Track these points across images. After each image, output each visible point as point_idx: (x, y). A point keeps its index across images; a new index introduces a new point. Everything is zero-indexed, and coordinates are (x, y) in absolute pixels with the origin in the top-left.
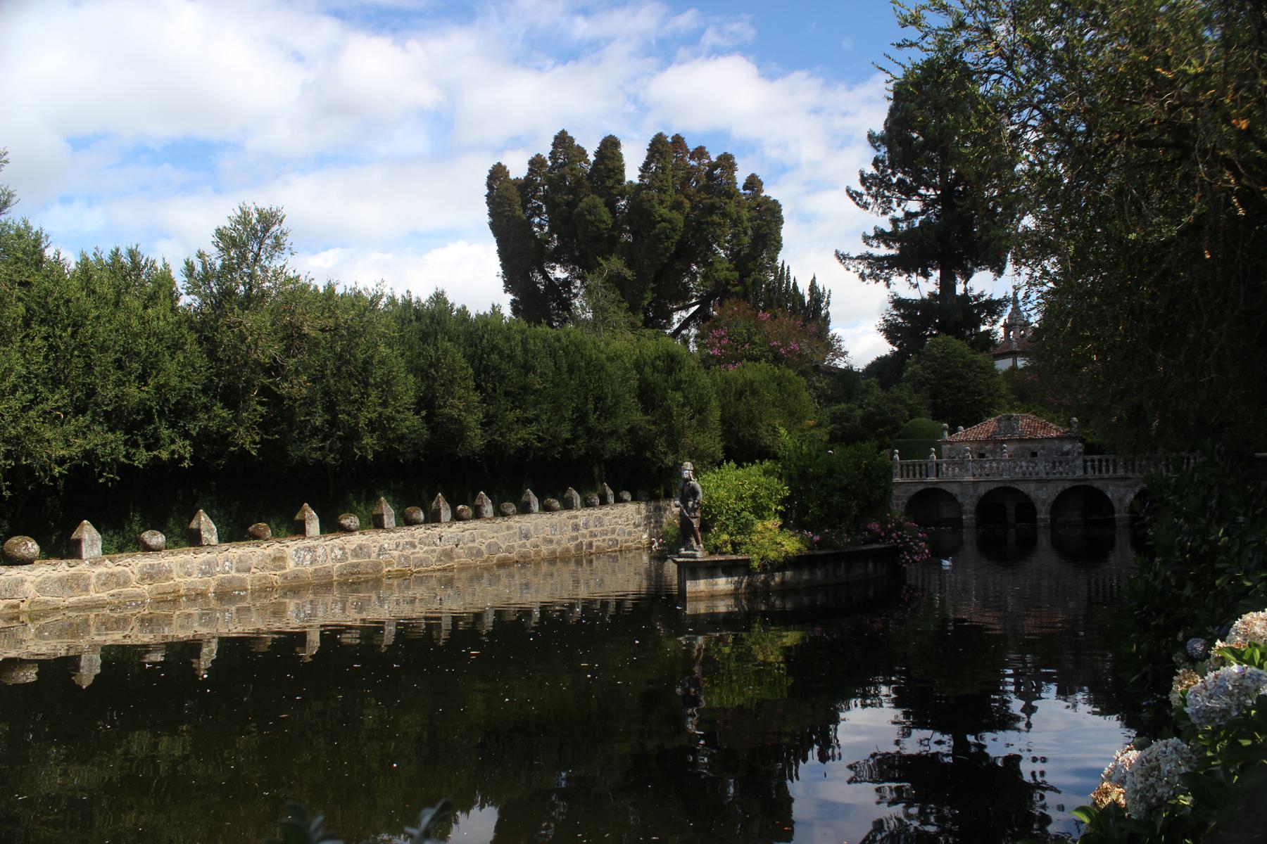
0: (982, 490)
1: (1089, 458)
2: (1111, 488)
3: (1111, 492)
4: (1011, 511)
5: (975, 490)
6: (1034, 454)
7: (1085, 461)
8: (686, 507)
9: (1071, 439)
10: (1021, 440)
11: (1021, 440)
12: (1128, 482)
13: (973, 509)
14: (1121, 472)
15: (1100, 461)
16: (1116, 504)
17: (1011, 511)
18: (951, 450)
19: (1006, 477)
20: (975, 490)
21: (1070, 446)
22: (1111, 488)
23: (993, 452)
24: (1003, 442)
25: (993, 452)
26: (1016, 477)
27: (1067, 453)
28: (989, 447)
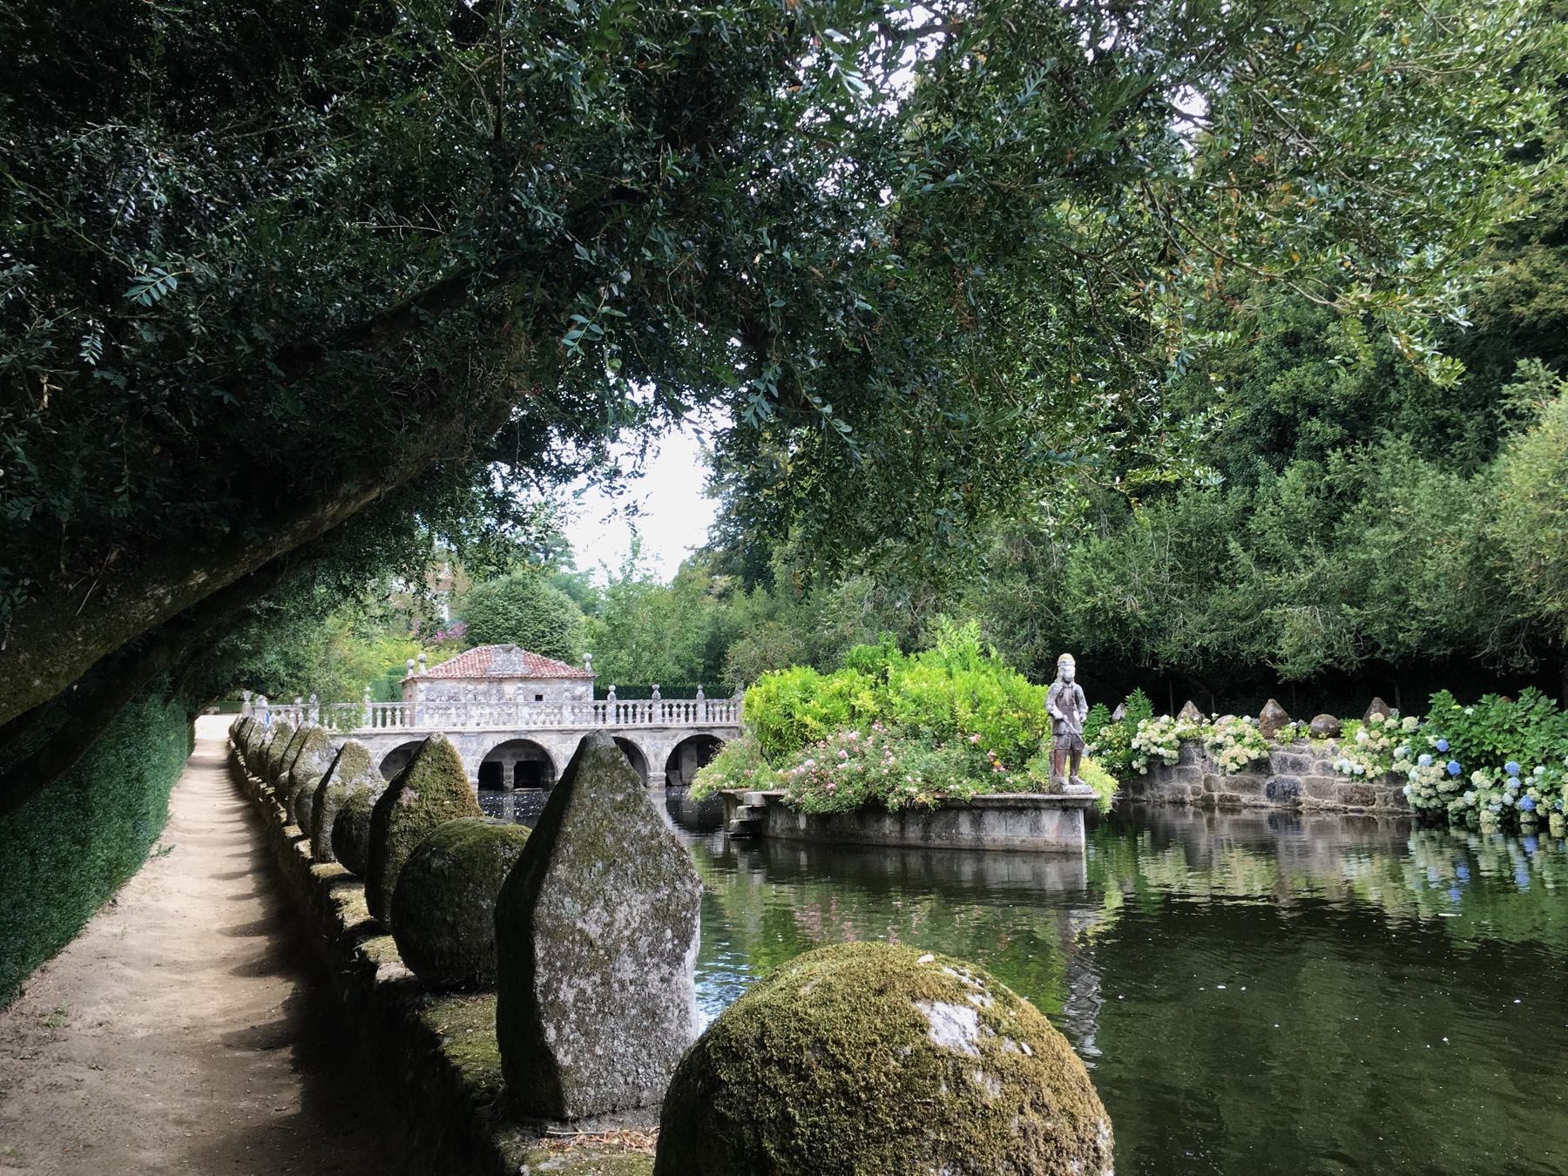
0: (489, 744)
1: (622, 703)
2: (647, 741)
3: (646, 745)
4: (509, 773)
5: (480, 744)
6: (539, 698)
7: (618, 707)
8: (1072, 719)
9: (585, 679)
10: (524, 679)
11: (524, 679)
12: (666, 733)
13: (477, 770)
14: (657, 722)
15: (634, 707)
16: (651, 761)
17: (509, 773)
18: (429, 690)
19: (525, 727)
20: (480, 744)
21: (584, 689)
22: (647, 741)
23: (485, 693)
24: (501, 680)
25: (485, 693)
26: (534, 728)
27: (580, 698)
28: (483, 687)
